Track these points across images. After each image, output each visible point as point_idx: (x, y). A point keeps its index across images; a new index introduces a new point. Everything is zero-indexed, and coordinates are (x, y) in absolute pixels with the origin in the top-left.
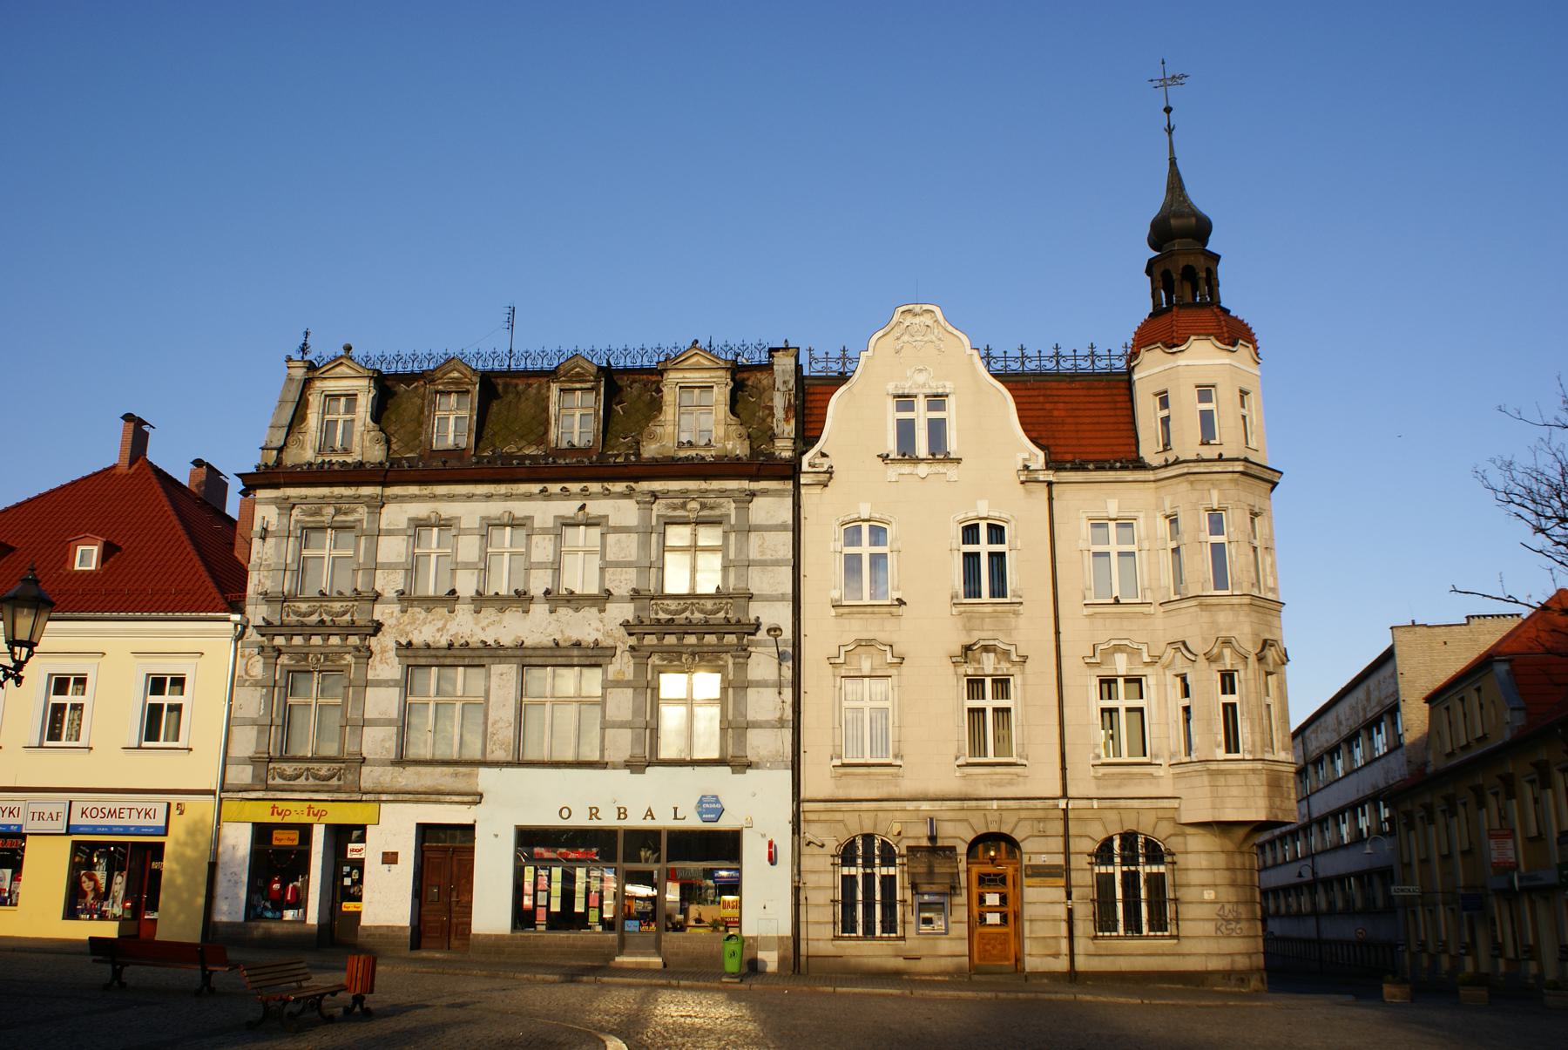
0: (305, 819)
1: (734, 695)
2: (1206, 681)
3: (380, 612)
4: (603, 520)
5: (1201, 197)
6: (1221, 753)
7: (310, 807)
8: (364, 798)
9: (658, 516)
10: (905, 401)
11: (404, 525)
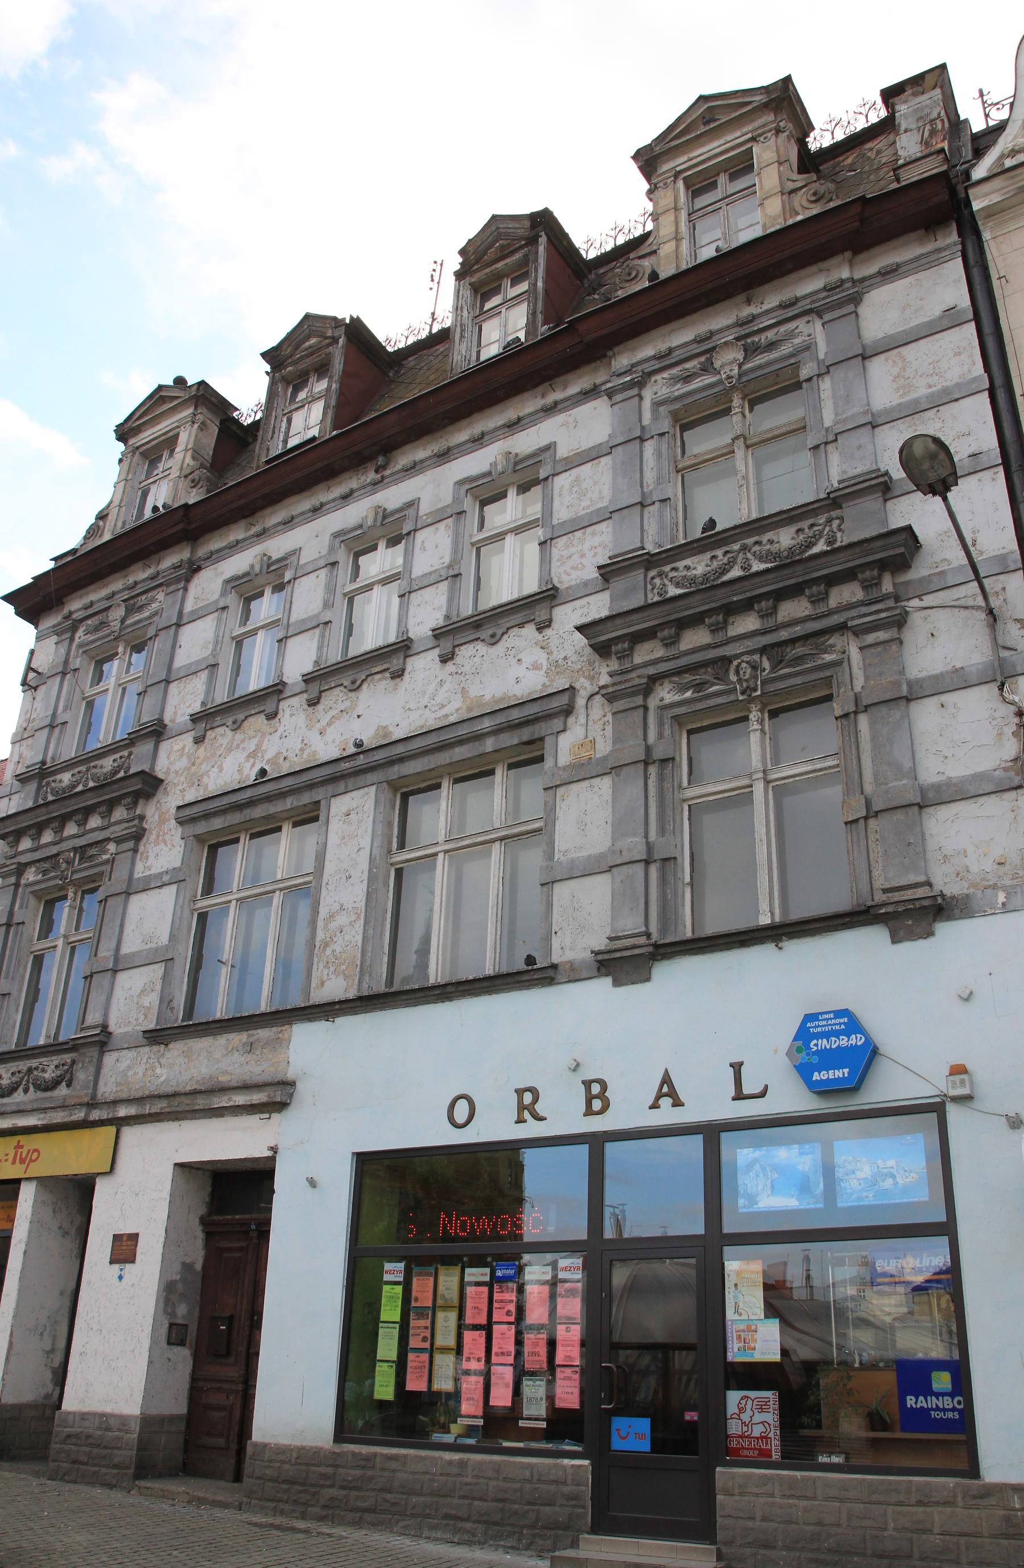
1: (872, 724)
4: (548, 454)
9: (657, 404)
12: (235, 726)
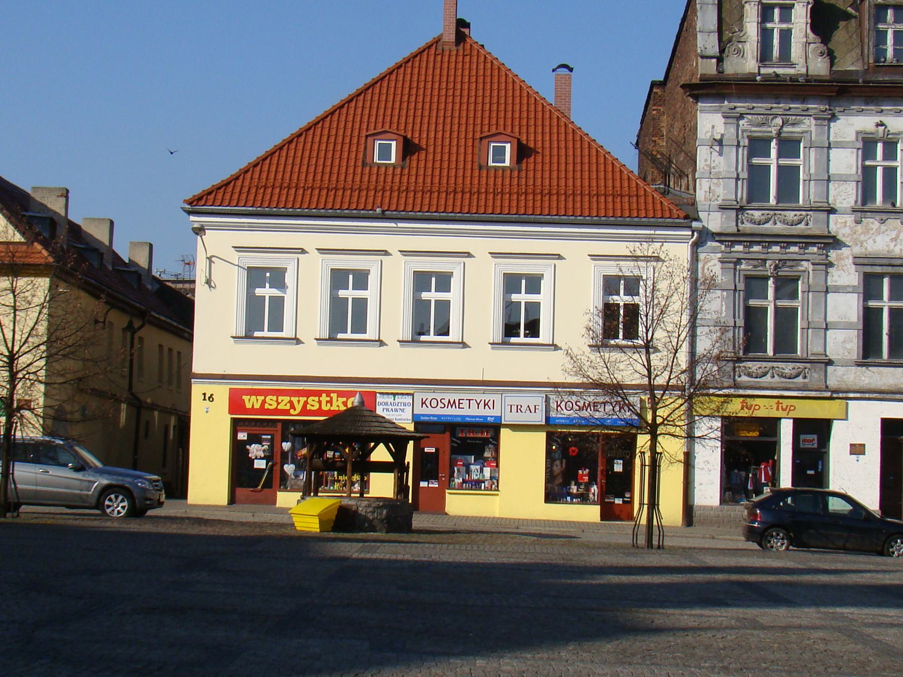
0: (774, 414)
3: (840, 225)
7: (778, 403)
8: (835, 395)
11: (852, 137)
12: (882, 222)
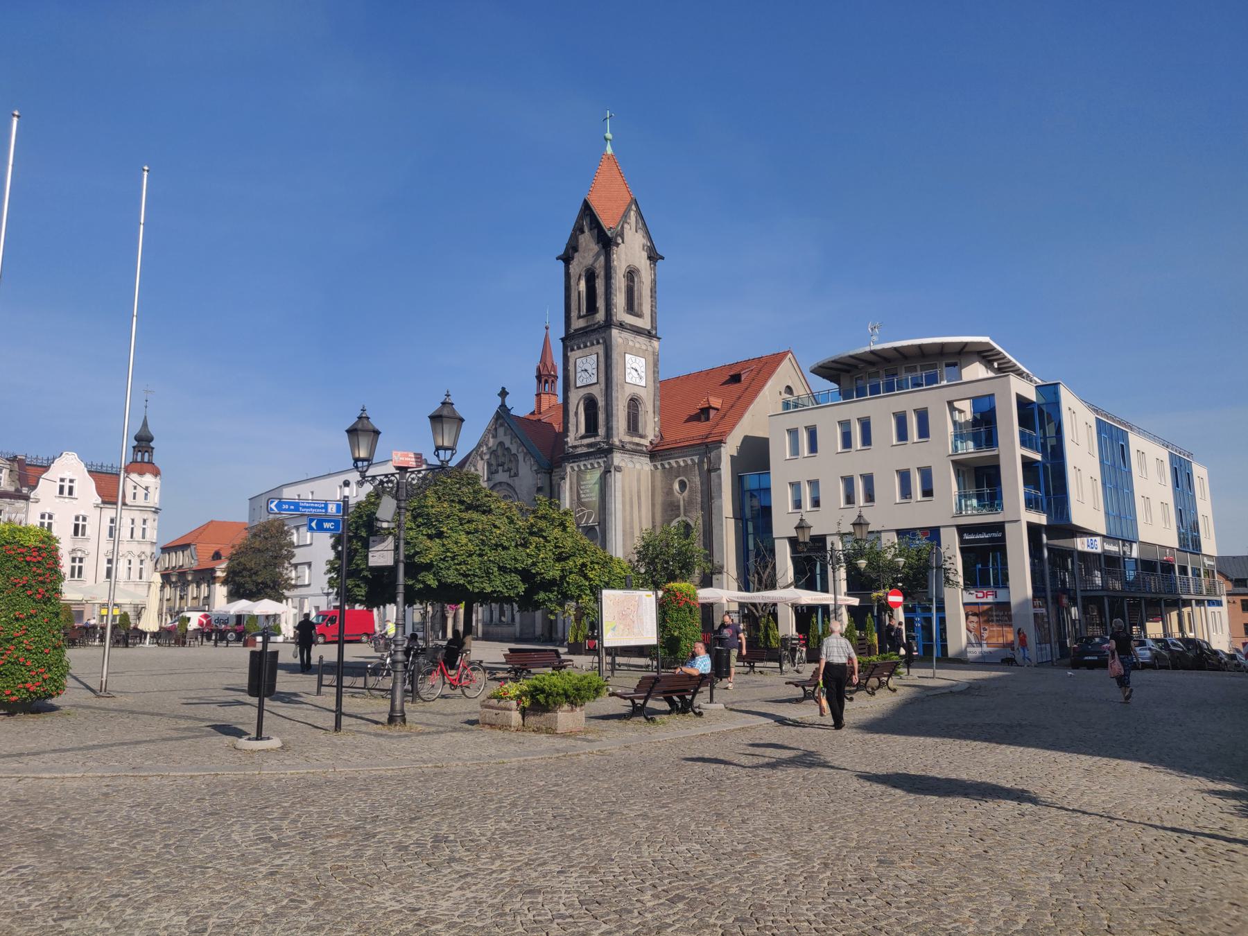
2: (136, 562)
5: (153, 429)
6: (138, 580)
10: (62, 480)
